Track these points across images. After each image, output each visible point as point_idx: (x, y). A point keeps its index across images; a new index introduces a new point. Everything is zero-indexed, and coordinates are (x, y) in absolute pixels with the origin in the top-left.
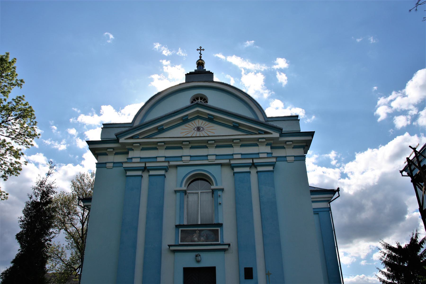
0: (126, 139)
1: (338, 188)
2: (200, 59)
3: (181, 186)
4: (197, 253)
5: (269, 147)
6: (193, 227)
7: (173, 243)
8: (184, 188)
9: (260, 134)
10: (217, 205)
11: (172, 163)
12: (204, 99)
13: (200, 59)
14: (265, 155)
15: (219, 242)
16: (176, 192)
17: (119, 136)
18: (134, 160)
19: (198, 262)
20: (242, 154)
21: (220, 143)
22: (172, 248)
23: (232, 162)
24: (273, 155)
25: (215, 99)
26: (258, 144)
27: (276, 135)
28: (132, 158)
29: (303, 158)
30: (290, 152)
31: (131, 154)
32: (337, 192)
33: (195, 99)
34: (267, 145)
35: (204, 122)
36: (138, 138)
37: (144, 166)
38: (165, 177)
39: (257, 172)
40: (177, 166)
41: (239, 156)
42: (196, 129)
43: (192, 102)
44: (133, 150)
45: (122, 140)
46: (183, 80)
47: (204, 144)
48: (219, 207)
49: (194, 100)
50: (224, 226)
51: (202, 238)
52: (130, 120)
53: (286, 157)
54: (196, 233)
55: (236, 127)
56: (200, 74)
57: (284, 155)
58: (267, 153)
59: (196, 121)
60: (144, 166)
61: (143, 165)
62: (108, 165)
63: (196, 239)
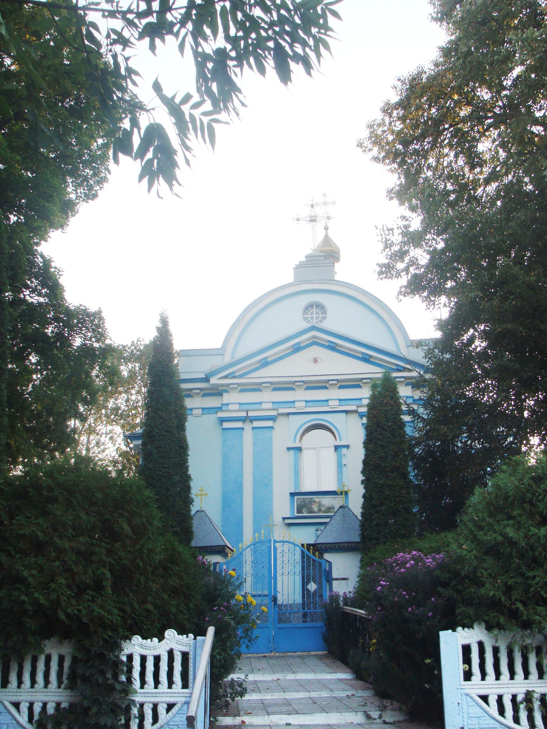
4: (317, 527)
5: (410, 387)
8: (297, 445)
11: (282, 411)
16: (289, 449)
18: (231, 407)
31: (227, 398)
34: (407, 385)
36: (234, 377)
37: (246, 415)
38: (274, 429)
40: (288, 414)
45: (214, 380)
46: (290, 278)
48: (344, 469)
49: (306, 308)
52: (217, 344)
55: (366, 359)
60: (246, 415)
61: (244, 414)
62: (194, 412)
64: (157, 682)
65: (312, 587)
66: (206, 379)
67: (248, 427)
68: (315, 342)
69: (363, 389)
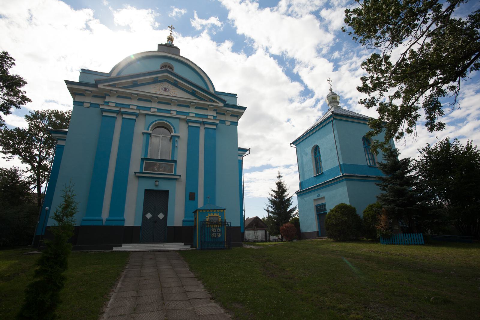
0: (104, 86)
1: (250, 148)
2: (171, 35)
3: (148, 130)
4: (156, 180)
6: (154, 161)
7: (138, 171)
9: (210, 101)
10: (174, 147)
11: (142, 112)
13: (171, 35)
14: (212, 118)
15: (173, 173)
16: (143, 133)
17: (98, 82)
19: (157, 186)
20: (196, 114)
21: (181, 104)
22: (137, 175)
23: (188, 118)
24: (217, 118)
25: (178, 69)
26: (208, 108)
27: (221, 105)
28: (108, 102)
29: (236, 124)
30: (228, 119)
32: (249, 151)
34: (214, 110)
35: (170, 85)
36: (115, 87)
38: (136, 121)
39: (205, 128)
40: (146, 115)
41: (194, 115)
42: (163, 89)
43: (161, 68)
44: (109, 96)
45: (100, 86)
46: (156, 49)
47: (168, 102)
48: (176, 149)
50: (178, 162)
51: (161, 169)
53: (225, 121)
54: (156, 165)
55: (193, 93)
56: (169, 48)
57: (224, 120)
58: (214, 116)
59: (164, 83)
61: (118, 109)
63: (156, 169)
65: (149, 216)
66: (95, 86)
68: (166, 80)
69: (191, 109)
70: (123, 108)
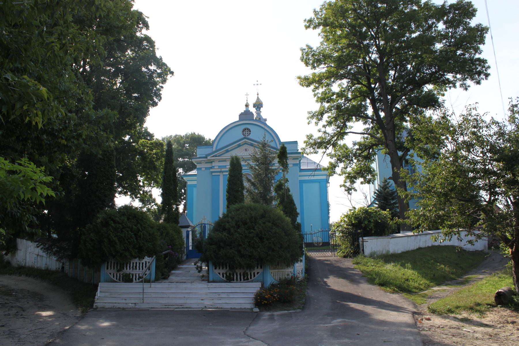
12: (249, 130)
31: (213, 164)
33: (244, 130)
45: (209, 158)
46: (237, 119)
59: (245, 145)
61: (220, 170)
64: (139, 269)
67: (221, 174)
68: (246, 143)
70: (223, 168)
